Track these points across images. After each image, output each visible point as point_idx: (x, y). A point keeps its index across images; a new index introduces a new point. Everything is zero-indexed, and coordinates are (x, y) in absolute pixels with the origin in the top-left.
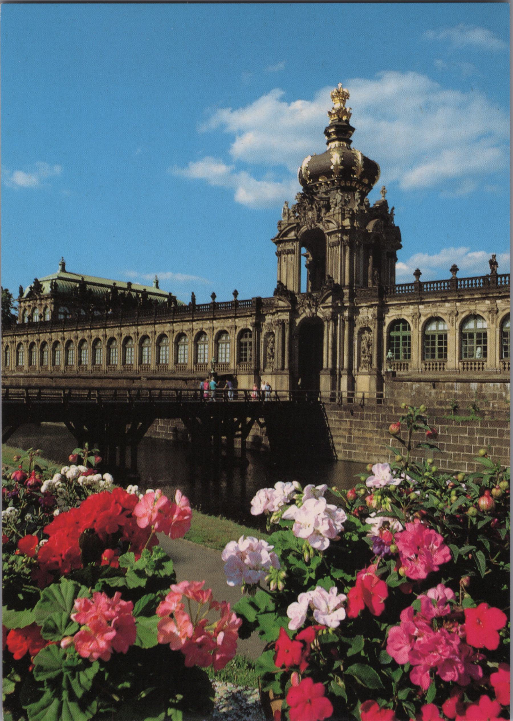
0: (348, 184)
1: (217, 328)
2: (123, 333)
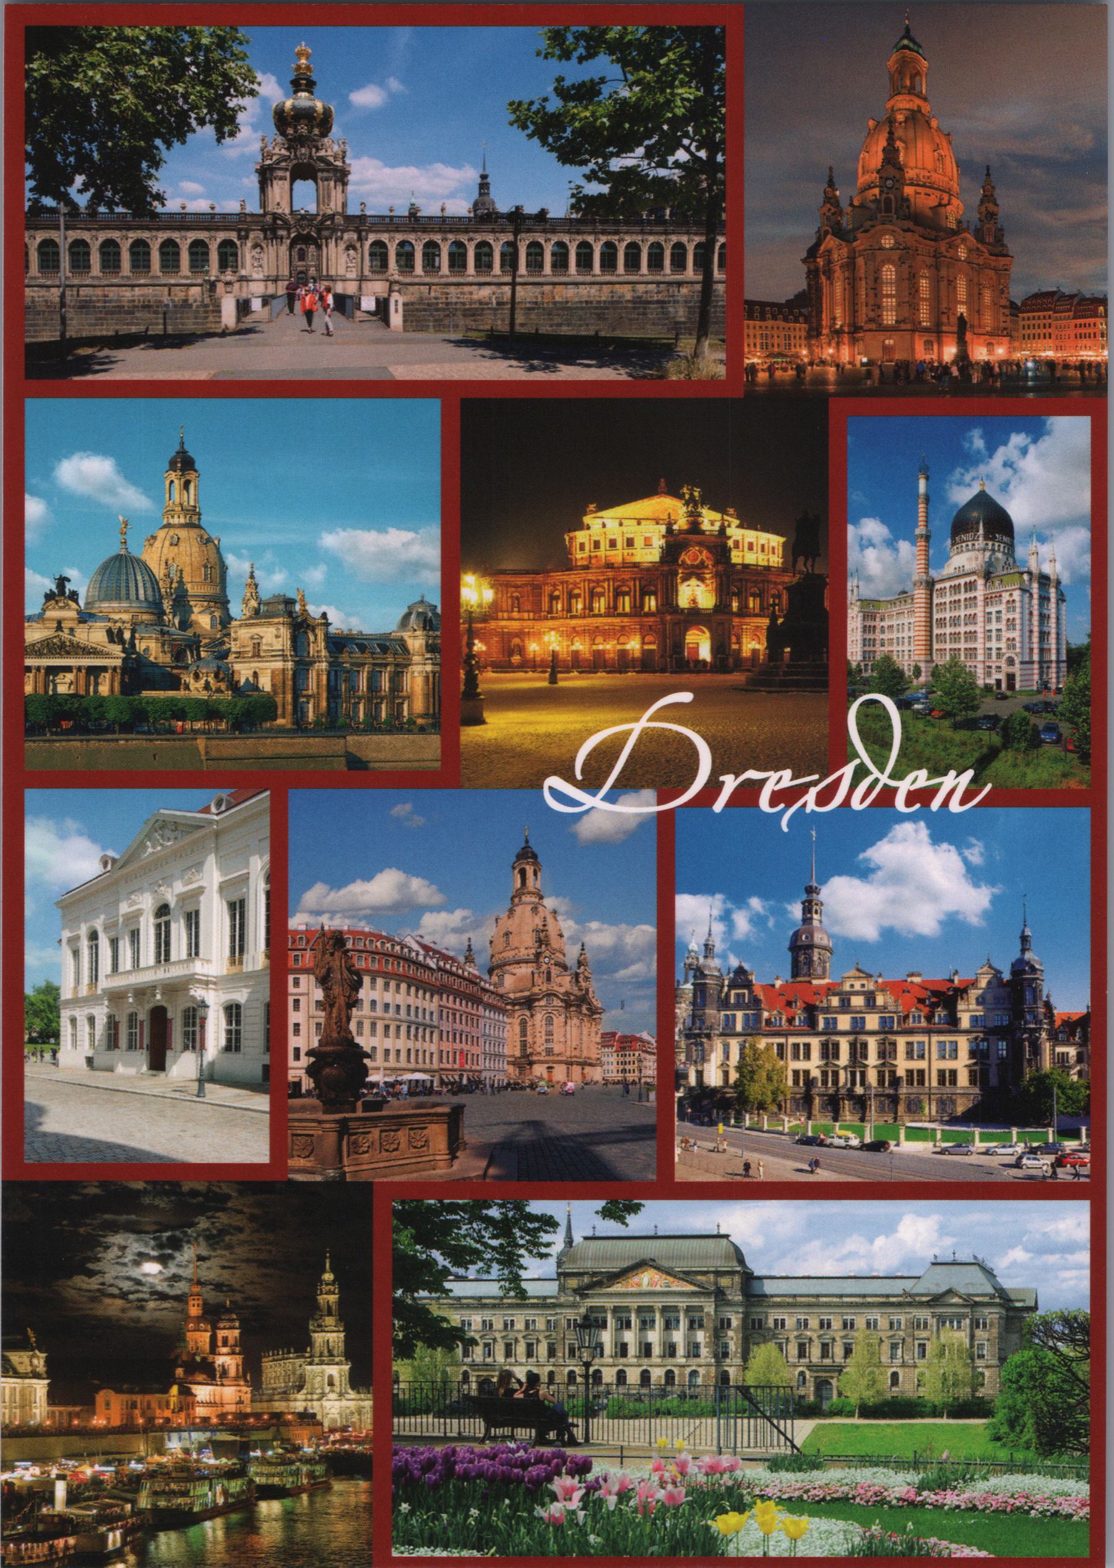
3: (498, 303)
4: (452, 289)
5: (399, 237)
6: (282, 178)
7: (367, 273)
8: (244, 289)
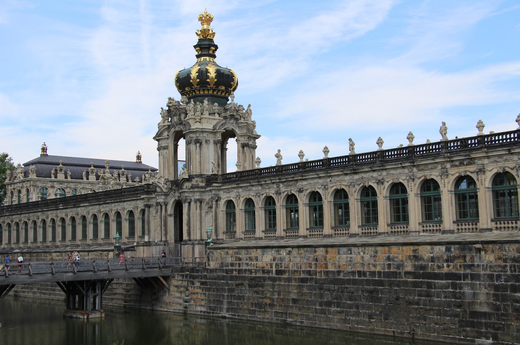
0: (206, 92)
1: (126, 209)
2: (69, 214)
3: (278, 272)
4: (243, 254)
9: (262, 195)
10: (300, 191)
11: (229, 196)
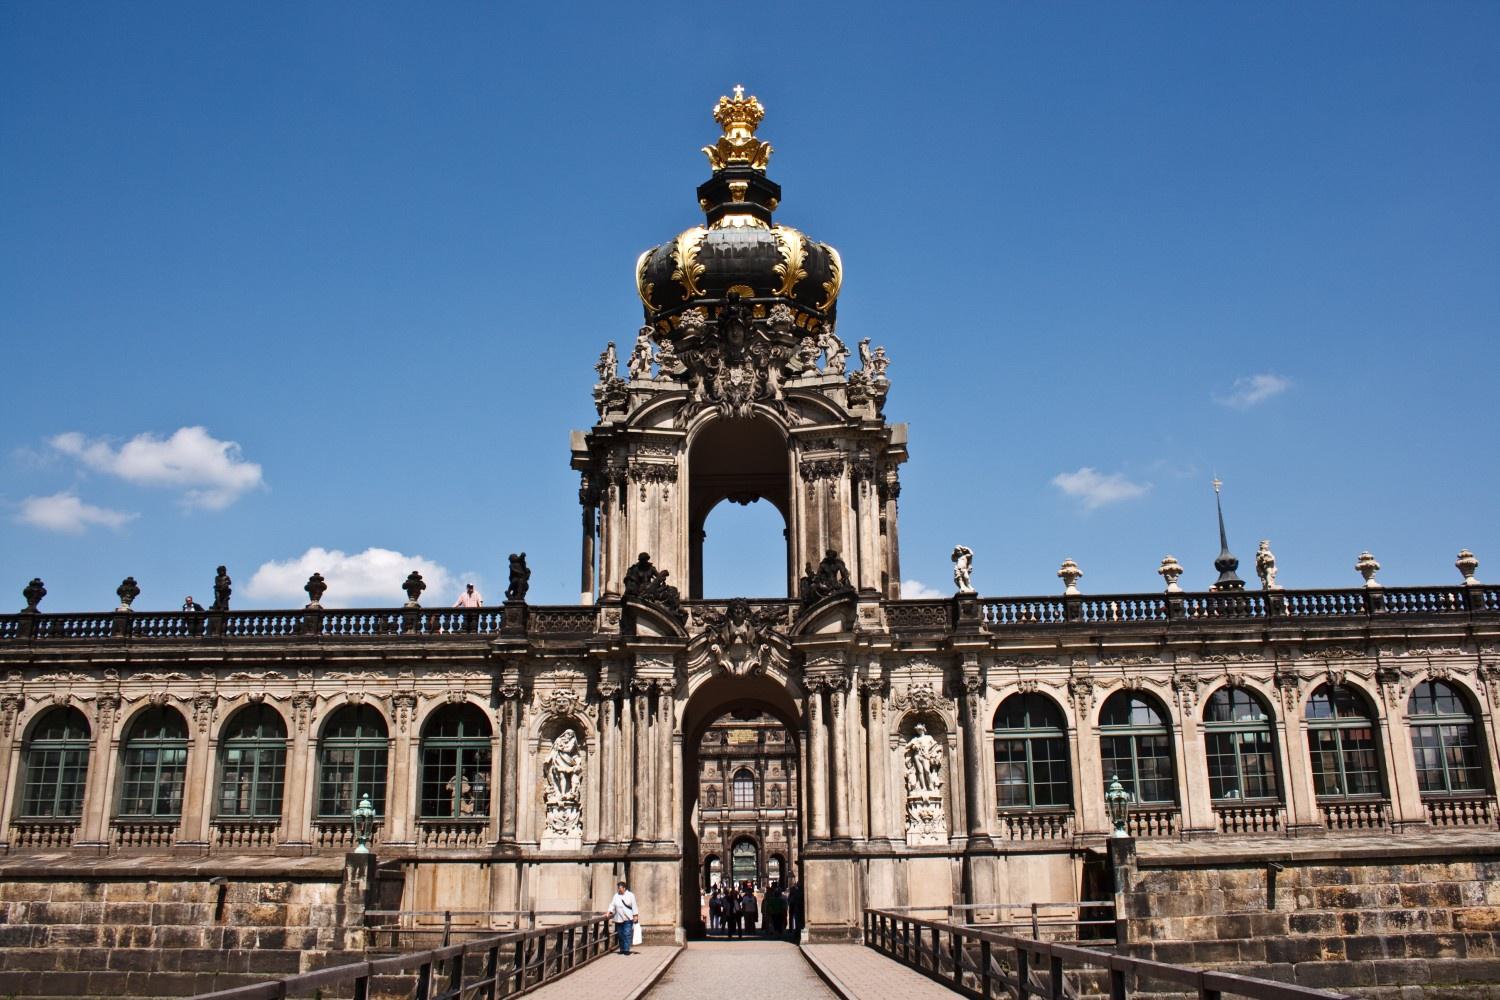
4: (1369, 882)
5: (1109, 678)
6: (668, 474)
7: (990, 824)
8: (506, 900)
9: (1207, 682)
10: (1386, 676)
11: (1033, 677)
